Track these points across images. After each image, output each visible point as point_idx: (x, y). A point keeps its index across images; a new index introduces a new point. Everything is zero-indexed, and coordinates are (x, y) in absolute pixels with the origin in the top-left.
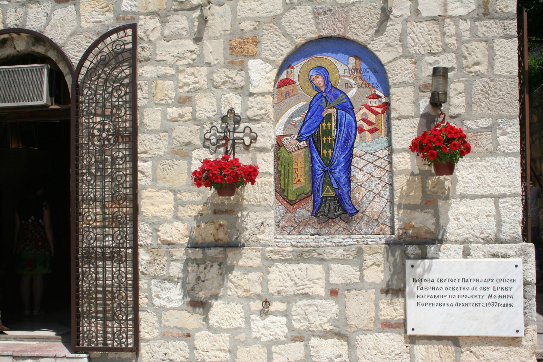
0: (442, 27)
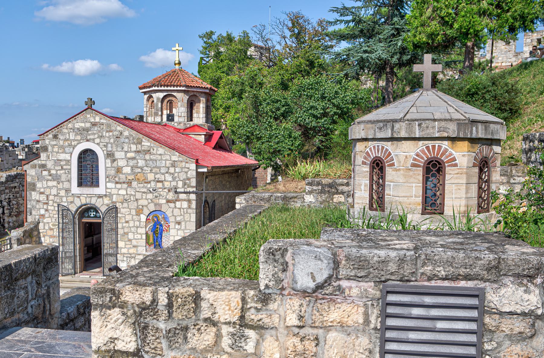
0: (180, 211)
